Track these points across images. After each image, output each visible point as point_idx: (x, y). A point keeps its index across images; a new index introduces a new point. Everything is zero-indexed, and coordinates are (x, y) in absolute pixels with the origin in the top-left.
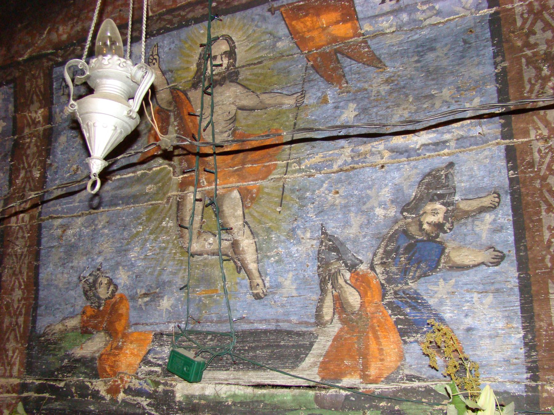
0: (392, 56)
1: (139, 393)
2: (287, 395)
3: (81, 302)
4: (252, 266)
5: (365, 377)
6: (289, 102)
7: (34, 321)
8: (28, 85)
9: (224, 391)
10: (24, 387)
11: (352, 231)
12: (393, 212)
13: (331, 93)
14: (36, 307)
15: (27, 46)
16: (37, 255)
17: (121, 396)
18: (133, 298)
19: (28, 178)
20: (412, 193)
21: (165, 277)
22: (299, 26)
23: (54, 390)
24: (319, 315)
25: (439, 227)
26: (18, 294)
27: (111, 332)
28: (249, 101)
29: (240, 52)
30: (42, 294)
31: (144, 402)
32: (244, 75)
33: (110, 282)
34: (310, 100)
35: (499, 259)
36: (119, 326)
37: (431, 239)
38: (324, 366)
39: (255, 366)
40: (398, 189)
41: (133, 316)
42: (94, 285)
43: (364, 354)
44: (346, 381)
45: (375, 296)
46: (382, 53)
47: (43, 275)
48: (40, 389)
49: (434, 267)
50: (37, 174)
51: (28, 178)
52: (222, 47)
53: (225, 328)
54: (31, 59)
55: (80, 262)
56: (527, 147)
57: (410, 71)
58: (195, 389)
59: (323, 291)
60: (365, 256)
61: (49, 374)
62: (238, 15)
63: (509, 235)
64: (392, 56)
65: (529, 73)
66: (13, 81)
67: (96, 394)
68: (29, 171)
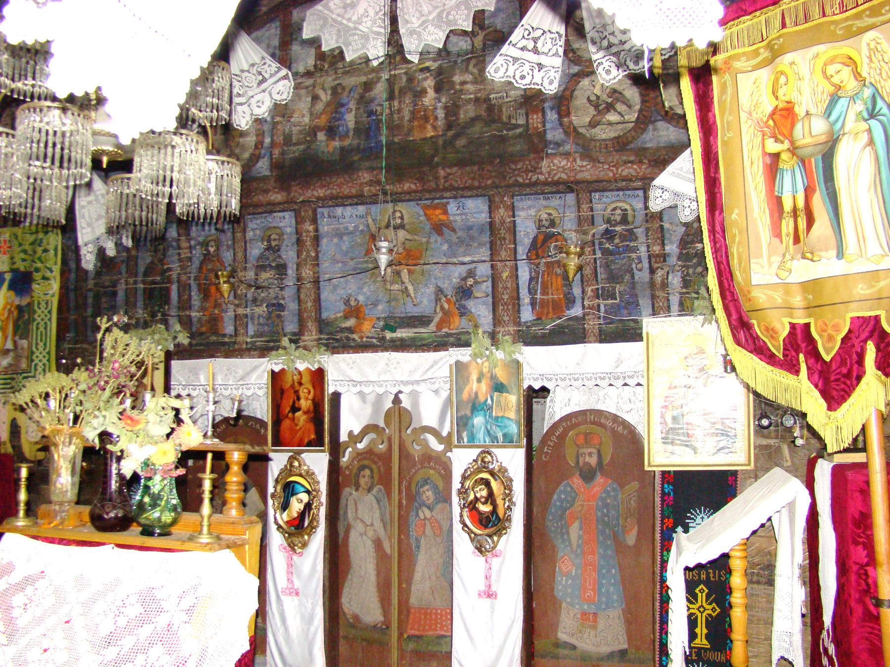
0: (460, 229)
1: (372, 338)
2: (425, 335)
3: (343, 307)
4: (413, 295)
5: (450, 329)
6: (424, 240)
7: (320, 314)
8: (303, 214)
9: (404, 335)
10: (320, 339)
11: (446, 286)
12: (458, 280)
13: (439, 239)
14: (320, 309)
15: (300, 195)
16: (319, 289)
17: (365, 339)
18: (366, 305)
19: (308, 256)
20: (464, 275)
21: (379, 298)
22: (428, 212)
23: (334, 339)
24: (435, 311)
25: (471, 286)
26: (310, 304)
27: (357, 317)
28: (409, 237)
29: (405, 217)
30: (323, 304)
31: (374, 341)
32: (407, 227)
33: (356, 300)
34: (432, 240)
35: (487, 296)
36: (361, 315)
37: (469, 289)
38: (437, 326)
39: (415, 327)
40: (460, 274)
41: (367, 312)
42: (348, 301)
43: (449, 322)
44: (444, 330)
45: (452, 305)
46: (456, 228)
47: (323, 297)
48: (328, 339)
49: (470, 297)
50: (313, 255)
51: (308, 256)
52: (398, 214)
53: (404, 315)
54: (303, 202)
55: (341, 292)
56: (496, 265)
57: (465, 236)
58: (394, 335)
59: (437, 304)
60: (449, 293)
61: (331, 334)
62: (404, 204)
63: (490, 289)
64: (460, 229)
65: (498, 243)
66: (294, 210)
67: (354, 340)
68: (308, 252)
